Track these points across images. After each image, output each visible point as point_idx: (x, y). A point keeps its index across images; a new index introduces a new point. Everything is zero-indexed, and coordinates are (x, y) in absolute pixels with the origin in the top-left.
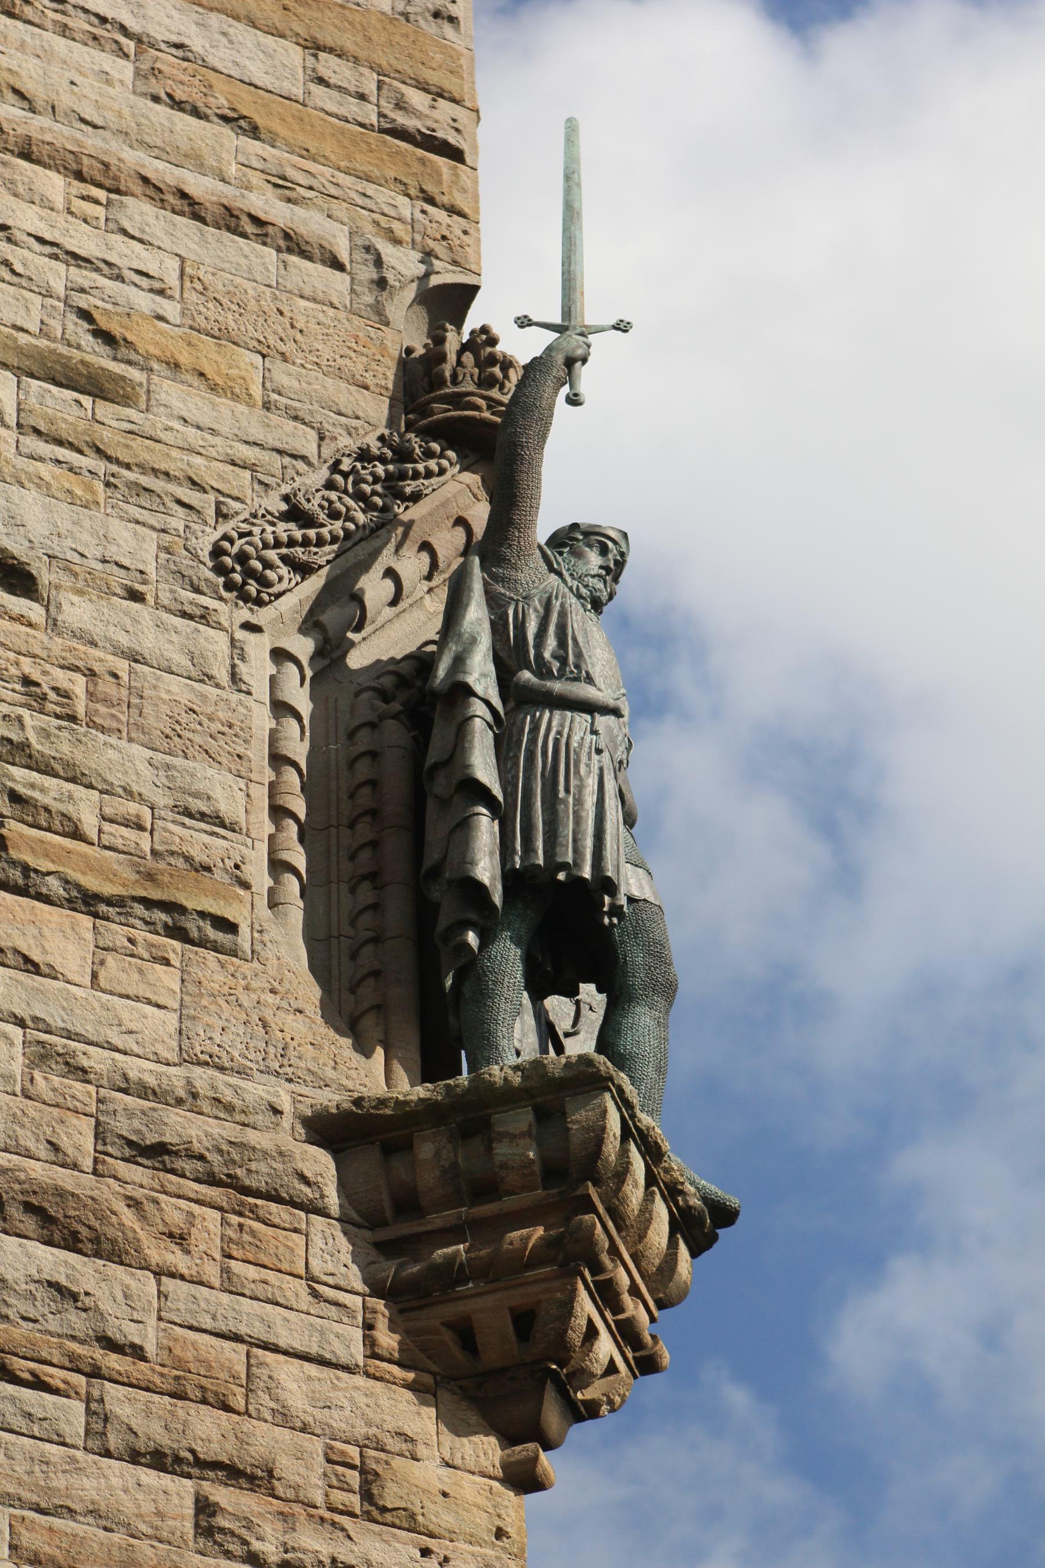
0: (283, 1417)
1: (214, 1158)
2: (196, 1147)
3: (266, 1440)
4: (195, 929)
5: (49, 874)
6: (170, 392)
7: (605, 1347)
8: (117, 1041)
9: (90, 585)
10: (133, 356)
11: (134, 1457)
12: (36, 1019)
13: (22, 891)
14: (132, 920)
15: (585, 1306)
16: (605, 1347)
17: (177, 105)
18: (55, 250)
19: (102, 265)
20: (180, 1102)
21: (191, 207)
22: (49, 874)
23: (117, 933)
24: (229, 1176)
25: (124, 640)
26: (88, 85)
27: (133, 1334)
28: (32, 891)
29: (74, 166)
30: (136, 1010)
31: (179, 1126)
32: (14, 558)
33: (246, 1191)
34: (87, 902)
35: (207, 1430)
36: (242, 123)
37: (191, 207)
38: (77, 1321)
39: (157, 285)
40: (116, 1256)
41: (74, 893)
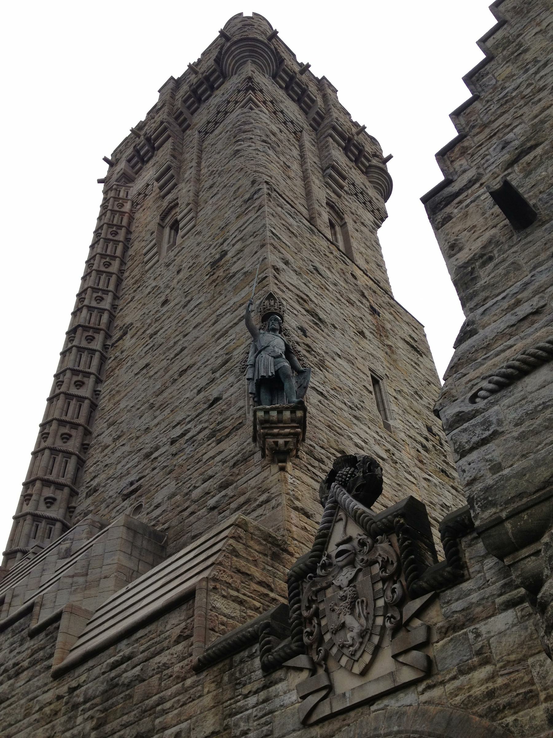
0: (252, 488)
3: (247, 495)
6: (235, 353)
7: (281, 441)
11: (235, 511)
15: (271, 441)
16: (281, 441)
21: (236, 324)
23: (230, 437)
27: (232, 494)
30: (231, 447)
31: (236, 458)
34: (227, 436)
35: (242, 499)
37: (236, 324)
38: (227, 498)
40: (231, 484)
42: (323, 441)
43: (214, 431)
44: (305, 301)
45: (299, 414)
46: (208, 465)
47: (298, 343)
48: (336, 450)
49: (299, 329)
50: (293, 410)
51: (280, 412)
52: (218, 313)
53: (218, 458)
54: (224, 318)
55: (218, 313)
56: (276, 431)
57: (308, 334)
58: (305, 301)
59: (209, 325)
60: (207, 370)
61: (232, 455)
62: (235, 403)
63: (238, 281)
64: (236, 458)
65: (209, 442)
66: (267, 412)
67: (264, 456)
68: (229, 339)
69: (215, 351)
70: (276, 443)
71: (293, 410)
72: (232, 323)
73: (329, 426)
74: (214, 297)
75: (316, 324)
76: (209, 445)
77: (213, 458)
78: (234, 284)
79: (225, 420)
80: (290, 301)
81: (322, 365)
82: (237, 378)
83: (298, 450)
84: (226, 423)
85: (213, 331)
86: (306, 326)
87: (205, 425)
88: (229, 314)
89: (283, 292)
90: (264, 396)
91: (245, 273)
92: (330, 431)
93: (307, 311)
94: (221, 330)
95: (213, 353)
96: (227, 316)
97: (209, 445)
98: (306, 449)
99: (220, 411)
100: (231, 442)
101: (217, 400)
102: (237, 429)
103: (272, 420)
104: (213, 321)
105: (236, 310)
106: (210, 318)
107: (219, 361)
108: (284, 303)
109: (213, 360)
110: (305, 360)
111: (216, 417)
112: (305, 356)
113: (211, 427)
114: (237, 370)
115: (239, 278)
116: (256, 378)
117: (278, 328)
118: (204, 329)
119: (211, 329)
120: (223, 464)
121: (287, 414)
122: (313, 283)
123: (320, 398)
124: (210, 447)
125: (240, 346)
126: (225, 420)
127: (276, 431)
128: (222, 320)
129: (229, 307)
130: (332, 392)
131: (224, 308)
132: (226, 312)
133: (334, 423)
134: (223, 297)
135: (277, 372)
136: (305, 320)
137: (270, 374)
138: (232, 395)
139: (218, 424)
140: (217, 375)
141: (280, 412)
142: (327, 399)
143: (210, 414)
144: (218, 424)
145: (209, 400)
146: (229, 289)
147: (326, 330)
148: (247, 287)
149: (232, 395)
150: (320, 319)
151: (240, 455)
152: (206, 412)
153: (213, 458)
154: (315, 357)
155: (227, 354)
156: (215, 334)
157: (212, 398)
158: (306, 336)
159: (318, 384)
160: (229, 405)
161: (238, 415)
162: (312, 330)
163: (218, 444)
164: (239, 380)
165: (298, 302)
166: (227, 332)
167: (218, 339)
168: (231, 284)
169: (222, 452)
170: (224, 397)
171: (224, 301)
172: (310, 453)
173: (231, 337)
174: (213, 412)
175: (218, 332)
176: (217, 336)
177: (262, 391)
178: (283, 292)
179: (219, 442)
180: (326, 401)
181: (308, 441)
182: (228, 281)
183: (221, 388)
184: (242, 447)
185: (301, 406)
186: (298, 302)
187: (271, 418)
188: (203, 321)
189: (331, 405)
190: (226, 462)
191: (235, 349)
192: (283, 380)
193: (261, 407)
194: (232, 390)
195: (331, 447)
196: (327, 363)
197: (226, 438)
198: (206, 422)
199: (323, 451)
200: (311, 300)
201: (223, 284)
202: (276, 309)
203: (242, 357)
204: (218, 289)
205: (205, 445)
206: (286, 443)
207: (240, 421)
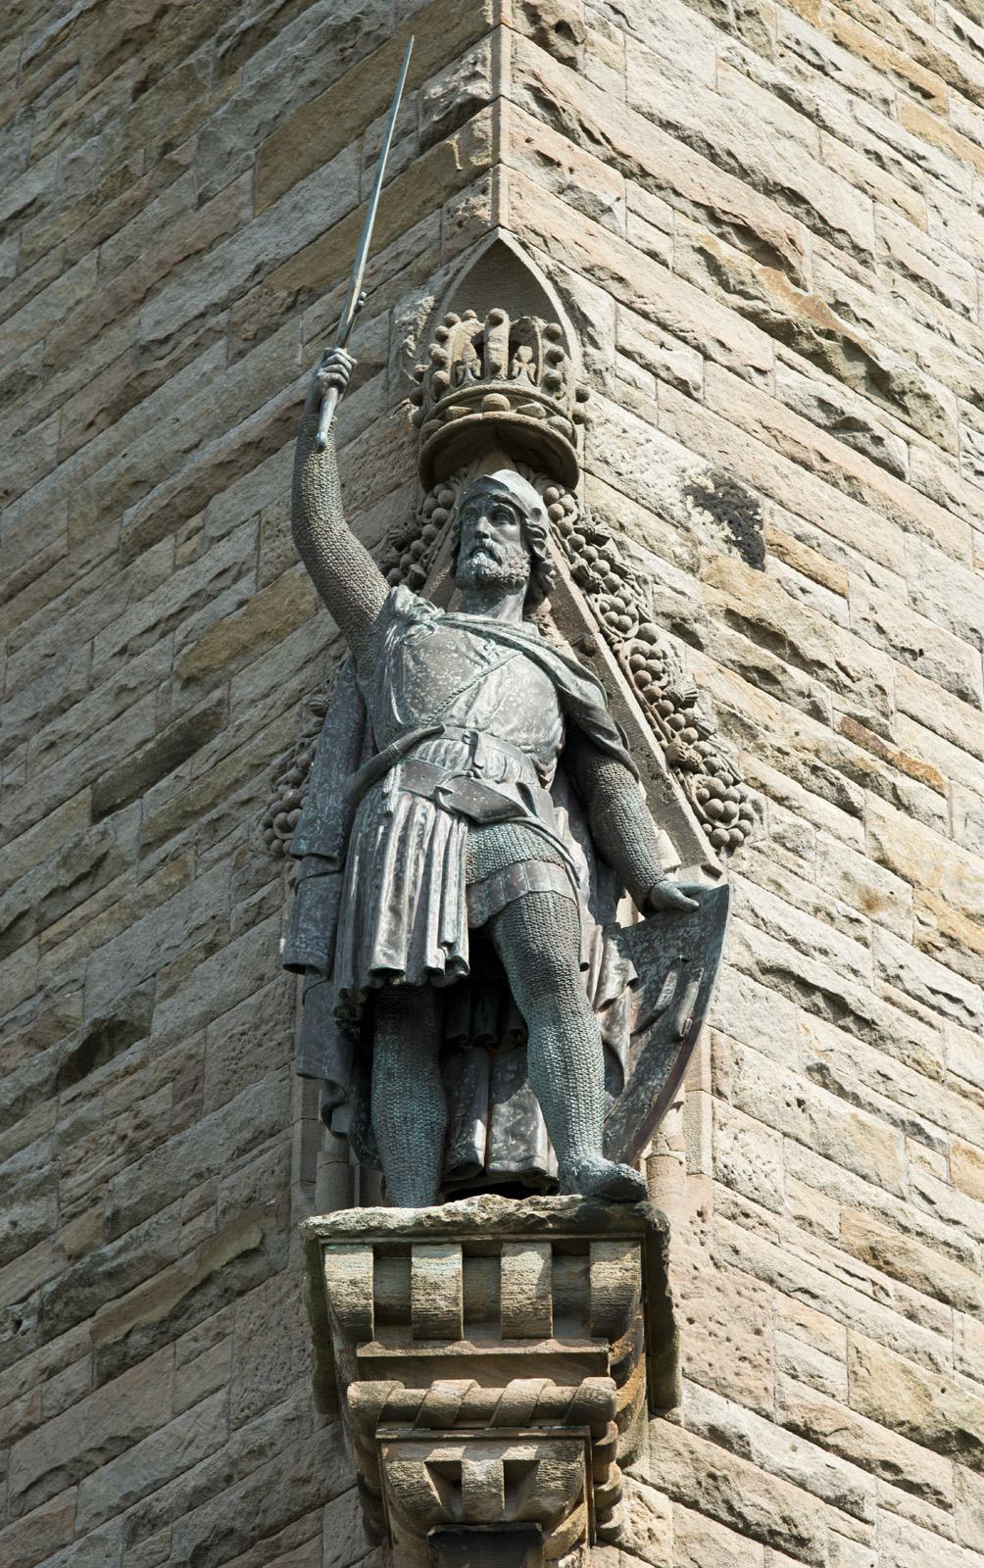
1: (238, 1524)
2: (225, 1524)
4: (235, 1281)
5: (128, 1335)
6: (245, 686)
7: (481, 1468)
8: (185, 1461)
9: (168, 977)
10: (213, 678)
12: (127, 1496)
13: (123, 1367)
14: (198, 1316)
16: (481, 1468)
17: (256, 339)
18: (162, 626)
19: (193, 602)
20: (229, 1479)
22: (128, 1335)
24: (254, 1529)
25: (196, 1010)
26: (185, 412)
28: (128, 1360)
29: (175, 514)
31: (208, 1515)
32: (104, 1021)
33: (275, 1529)
34: (166, 1332)
36: (301, 298)
39: (234, 572)
41: (152, 1333)
42: (815, 1380)
43: (85, 1280)
44: (767, 252)
45: (613, 1271)
46: (40, 1524)
47: (680, 629)
48: (914, 1434)
49: (702, 498)
50: (571, 1245)
51: (483, 1251)
52: (150, 321)
53: (103, 1486)
54: (188, 376)
55: (150, 321)
56: (447, 1391)
57: (774, 524)
58: (767, 252)
59: (84, 406)
60: (62, 772)
61: (193, 1479)
62: (230, 1087)
63: (288, 89)
64: (208, 1515)
65: (57, 1348)
66: (392, 1250)
67: (378, 1535)
68: (208, 565)
69: (116, 637)
70: (449, 1475)
71: (571, 1245)
72: (234, 436)
73: (874, 1256)
74: (126, 177)
75: (845, 426)
76: (51, 1372)
77: (74, 1472)
78: (266, 110)
79: (156, 1202)
80: (647, 279)
81: (862, 771)
82: (246, 887)
83: (602, 1507)
84: (165, 1234)
85: (107, 474)
86: (757, 464)
87: (33, 1214)
88: (218, 349)
89: (598, 212)
90: (404, 1103)
91: (337, 34)
92: (878, 1294)
93: (784, 332)
94: (164, 470)
95: (107, 644)
96: (206, 362)
97: (51, 1372)
98: (676, 1472)
99: (125, 1123)
100: (191, 1384)
101: (108, 1037)
102: (230, 1295)
103: (425, 1318)
104: (115, 379)
105: (268, 330)
106: (99, 355)
107: (140, 729)
108: (596, 303)
109: (97, 705)
110: (727, 749)
111: (102, 1164)
112: (733, 721)
113: (70, 1237)
114: (249, 828)
115: (298, 66)
116: (344, 980)
117: (521, 569)
118: (50, 433)
119: (102, 443)
120: (132, 1536)
121: (525, 1270)
122: (852, 69)
123: (826, 1034)
124: (58, 1385)
125: (277, 637)
126: (156, 1202)
127: (447, 1391)
128: (172, 387)
129: (219, 291)
130: (925, 973)
131: (190, 297)
132: (199, 331)
133: (918, 1216)
134: (183, 191)
135: (480, 937)
136: (757, 411)
137: (435, 958)
138: (209, 1017)
139: (115, 1225)
140: (126, 829)
141: (483, 1251)
142: (879, 1041)
143: (67, 1139)
144: (115, 1225)
145: (63, 1025)
146: (232, 141)
147: (921, 460)
148: (349, 155)
149: (209, 1017)
150: (879, 381)
151: (234, 1494)
152: (42, 1114)
153: (74, 1472)
154: (816, 713)
155: (189, 681)
156: (124, 502)
157: (84, 1011)
158: (754, 557)
159: (814, 931)
160: (190, 1089)
161: (230, 1188)
162: (807, 488)
163: (108, 1376)
164: (260, 912)
165: (714, 267)
166: (198, 498)
167: (143, 541)
168: (242, 107)
169: (129, 1442)
170: (160, 1025)
171: (190, 230)
172: (706, 1497)
173: (226, 553)
174: (81, 1127)
175: (142, 484)
176: (134, 514)
177: (387, 1058)
178: (598, 212)
179: (113, 1365)
180: (873, 1058)
181: (695, 1403)
182: (226, 67)
183: (143, 941)
184: (251, 1435)
185: (621, 1213)
186: (714, 267)
187: (420, 1301)
188: (50, 368)
189: (905, 1078)
190: (153, 1522)
191: (243, 651)
192: (518, 993)
193: (352, 1216)
194: (214, 979)
195: (877, 1416)
196: (906, 737)
197: (157, 1344)
198: (36, 1191)
199: (808, 1459)
200: (823, 229)
201: (190, 82)
202: (518, 398)
203: (288, 727)
204: (162, 113)
205: (26, 1368)
206: (517, 1475)
207: (251, 1240)
